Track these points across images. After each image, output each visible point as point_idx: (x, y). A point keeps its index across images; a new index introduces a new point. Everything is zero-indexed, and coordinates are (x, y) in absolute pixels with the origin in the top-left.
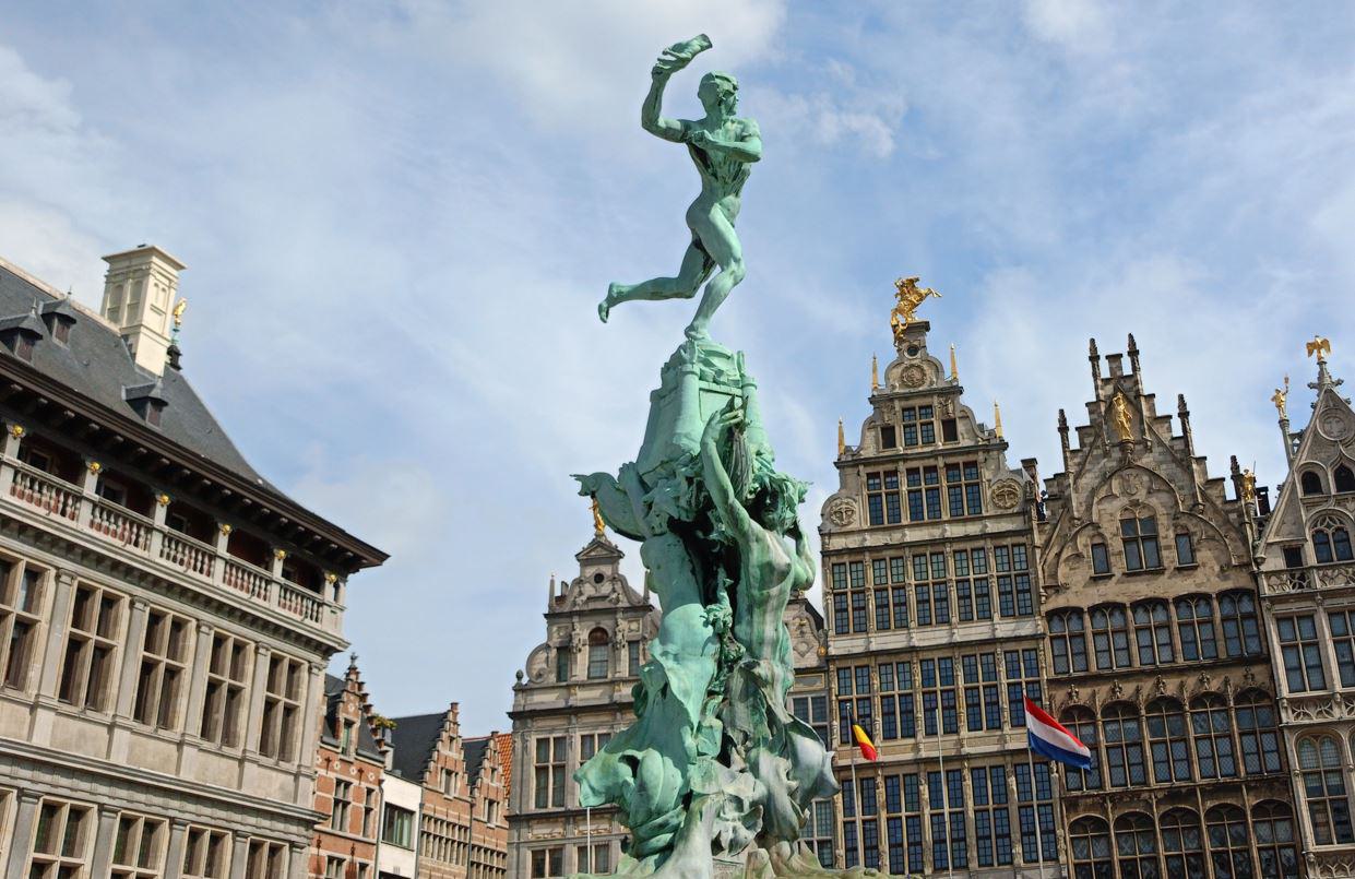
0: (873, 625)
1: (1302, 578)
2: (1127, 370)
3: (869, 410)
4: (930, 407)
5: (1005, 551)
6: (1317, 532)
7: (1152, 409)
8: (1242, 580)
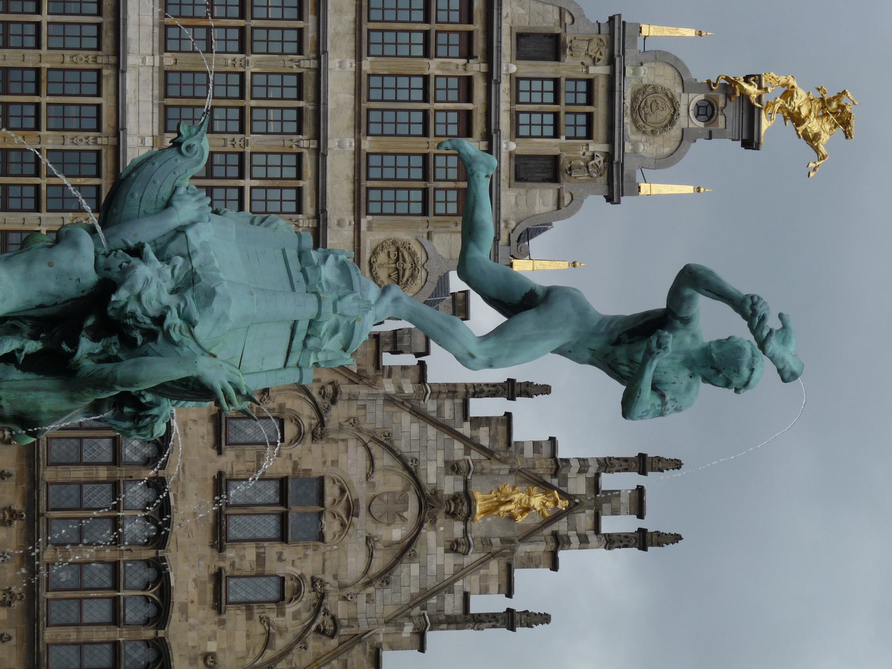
2: (611, 524)
4: (589, 136)
7: (530, 562)
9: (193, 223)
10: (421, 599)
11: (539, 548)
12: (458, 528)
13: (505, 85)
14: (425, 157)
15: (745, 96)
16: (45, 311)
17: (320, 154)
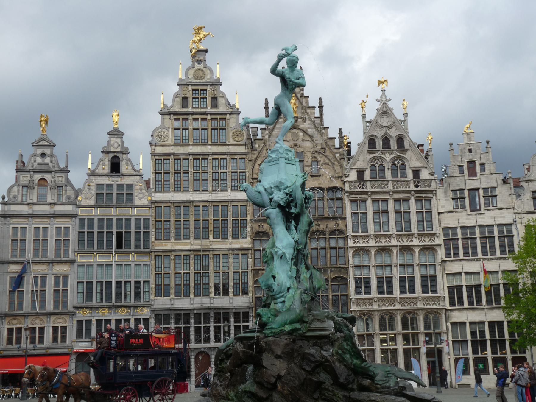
0: (172, 189)
1: (363, 185)
3: (176, 89)
4: (206, 90)
5: (235, 160)
6: (372, 165)
7: (307, 102)
8: (337, 183)
9: (263, 187)
10: (316, 128)
11: (304, 100)
12: (299, 120)
13: (195, 110)
14: (212, 129)
15: (195, 53)
16: (285, 220)
17: (212, 154)
